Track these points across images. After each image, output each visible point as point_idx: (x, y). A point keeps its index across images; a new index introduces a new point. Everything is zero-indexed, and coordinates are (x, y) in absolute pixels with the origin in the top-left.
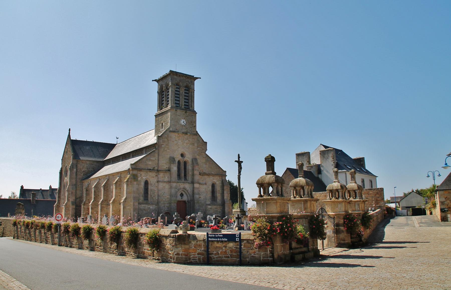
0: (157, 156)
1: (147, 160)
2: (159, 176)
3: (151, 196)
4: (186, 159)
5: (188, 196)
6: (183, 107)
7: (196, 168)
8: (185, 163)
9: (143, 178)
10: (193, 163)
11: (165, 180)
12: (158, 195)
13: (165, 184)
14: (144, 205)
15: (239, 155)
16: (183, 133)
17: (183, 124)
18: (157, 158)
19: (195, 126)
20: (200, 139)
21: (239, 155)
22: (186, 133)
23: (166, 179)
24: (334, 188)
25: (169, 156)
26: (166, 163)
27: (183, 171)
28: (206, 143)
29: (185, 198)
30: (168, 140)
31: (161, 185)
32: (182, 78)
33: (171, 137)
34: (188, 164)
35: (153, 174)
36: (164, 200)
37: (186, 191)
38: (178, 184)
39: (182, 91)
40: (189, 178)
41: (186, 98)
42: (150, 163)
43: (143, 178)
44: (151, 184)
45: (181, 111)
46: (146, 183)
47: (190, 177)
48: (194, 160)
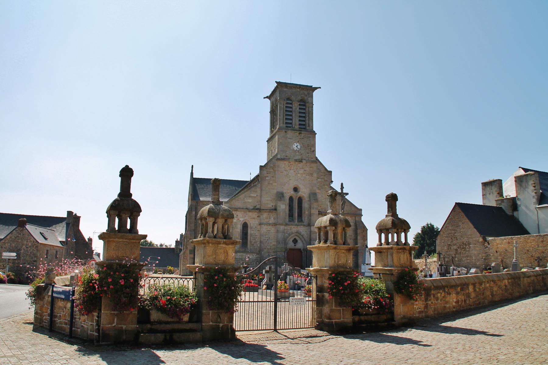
0: (259, 192)
1: (245, 197)
2: (261, 217)
3: (251, 242)
4: (300, 194)
5: (304, 242)
6: (297, 127)
7: (315, 205)
8: (300, 200)
9: (240, 219)
10: (310, 200)
11: (271, 222)
12: (261, 242)
13: (269, 228)
14: (241, 254)
15: (342, 184)
16: (296, 160)
17: (296, 148)
18: (259, 194)
19: (314, 151)
20: (321, 167)
21: (342, 184)
22: (300, 161)
23: (272, 221)
24: (323, 225)
25: (275, 191)
26: (271, 201)
27: (297, 210)
28: (331, 172)
29: (300, 245)
30: (275, 171)
31: (264, 229)
32: (294, 90)
33: (278, 167)
34: (303, 201)
35: (254, 214)
36: (269, 247)
37: (301, 237)
38: (288, 228)
39: (296, 106)
40: (305, 219)
41: (301, 115)
42: (250, 201)
43: (240, 219)
44: (251, 228)
45: (293, 132)
46: (245, 226)
47: (306, 218)
48: (313, 196)
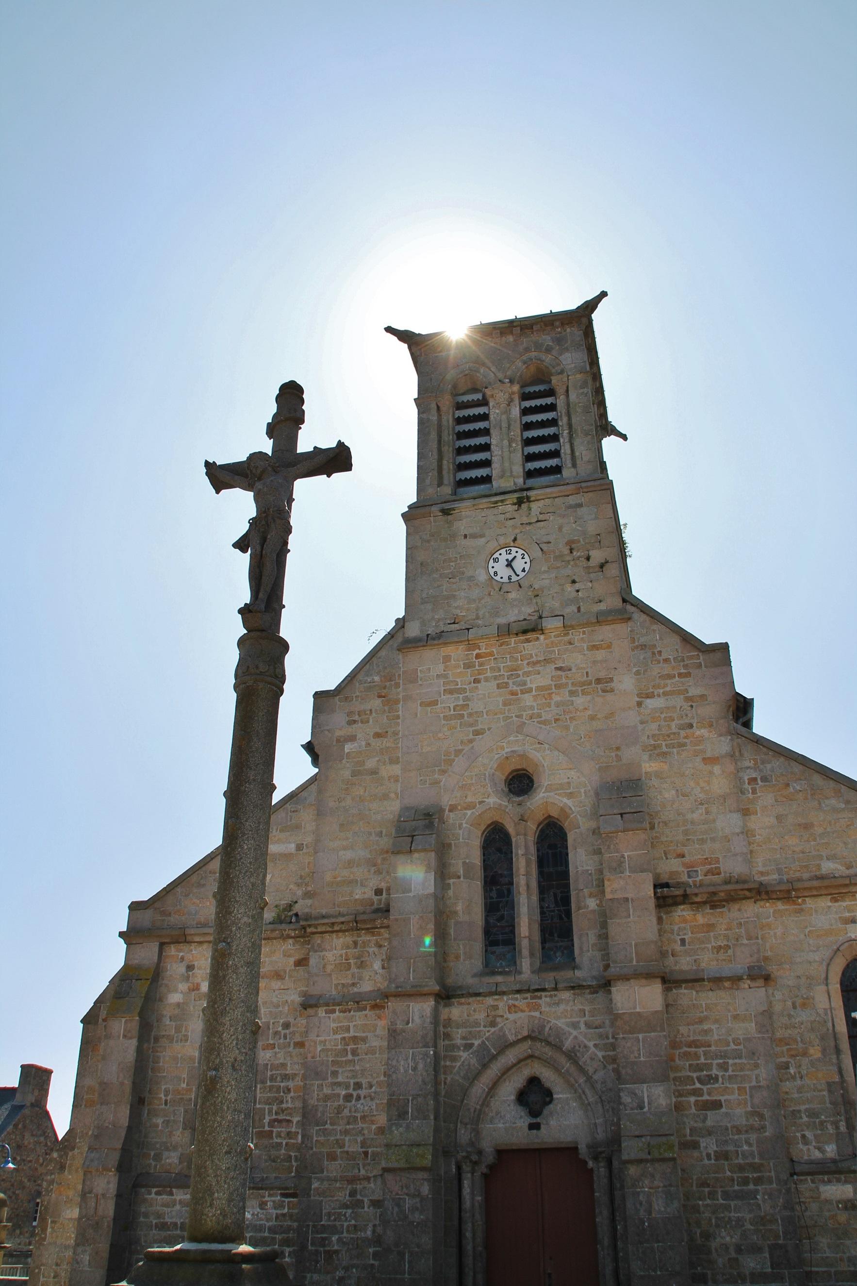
2: (312, 961)
4: (544, 799)
8: (552, 839)
11: (366, 987)
12: (308, 1115)
16: (506, 631)
22: (531, 628)
23: (371, 980)
25: (394, 807)
27: (529, 890)
28: (724, 648)
29: (568, 1122)
30: (390, 703)
31: (328, 1031)
36: (354, 1148)
